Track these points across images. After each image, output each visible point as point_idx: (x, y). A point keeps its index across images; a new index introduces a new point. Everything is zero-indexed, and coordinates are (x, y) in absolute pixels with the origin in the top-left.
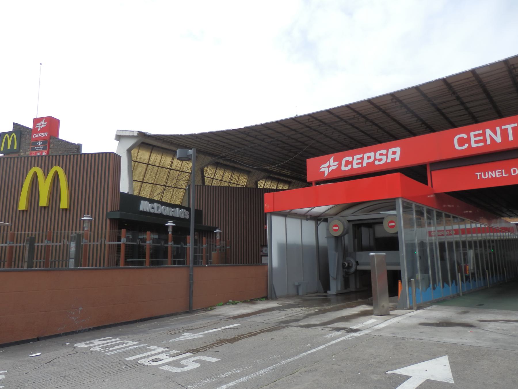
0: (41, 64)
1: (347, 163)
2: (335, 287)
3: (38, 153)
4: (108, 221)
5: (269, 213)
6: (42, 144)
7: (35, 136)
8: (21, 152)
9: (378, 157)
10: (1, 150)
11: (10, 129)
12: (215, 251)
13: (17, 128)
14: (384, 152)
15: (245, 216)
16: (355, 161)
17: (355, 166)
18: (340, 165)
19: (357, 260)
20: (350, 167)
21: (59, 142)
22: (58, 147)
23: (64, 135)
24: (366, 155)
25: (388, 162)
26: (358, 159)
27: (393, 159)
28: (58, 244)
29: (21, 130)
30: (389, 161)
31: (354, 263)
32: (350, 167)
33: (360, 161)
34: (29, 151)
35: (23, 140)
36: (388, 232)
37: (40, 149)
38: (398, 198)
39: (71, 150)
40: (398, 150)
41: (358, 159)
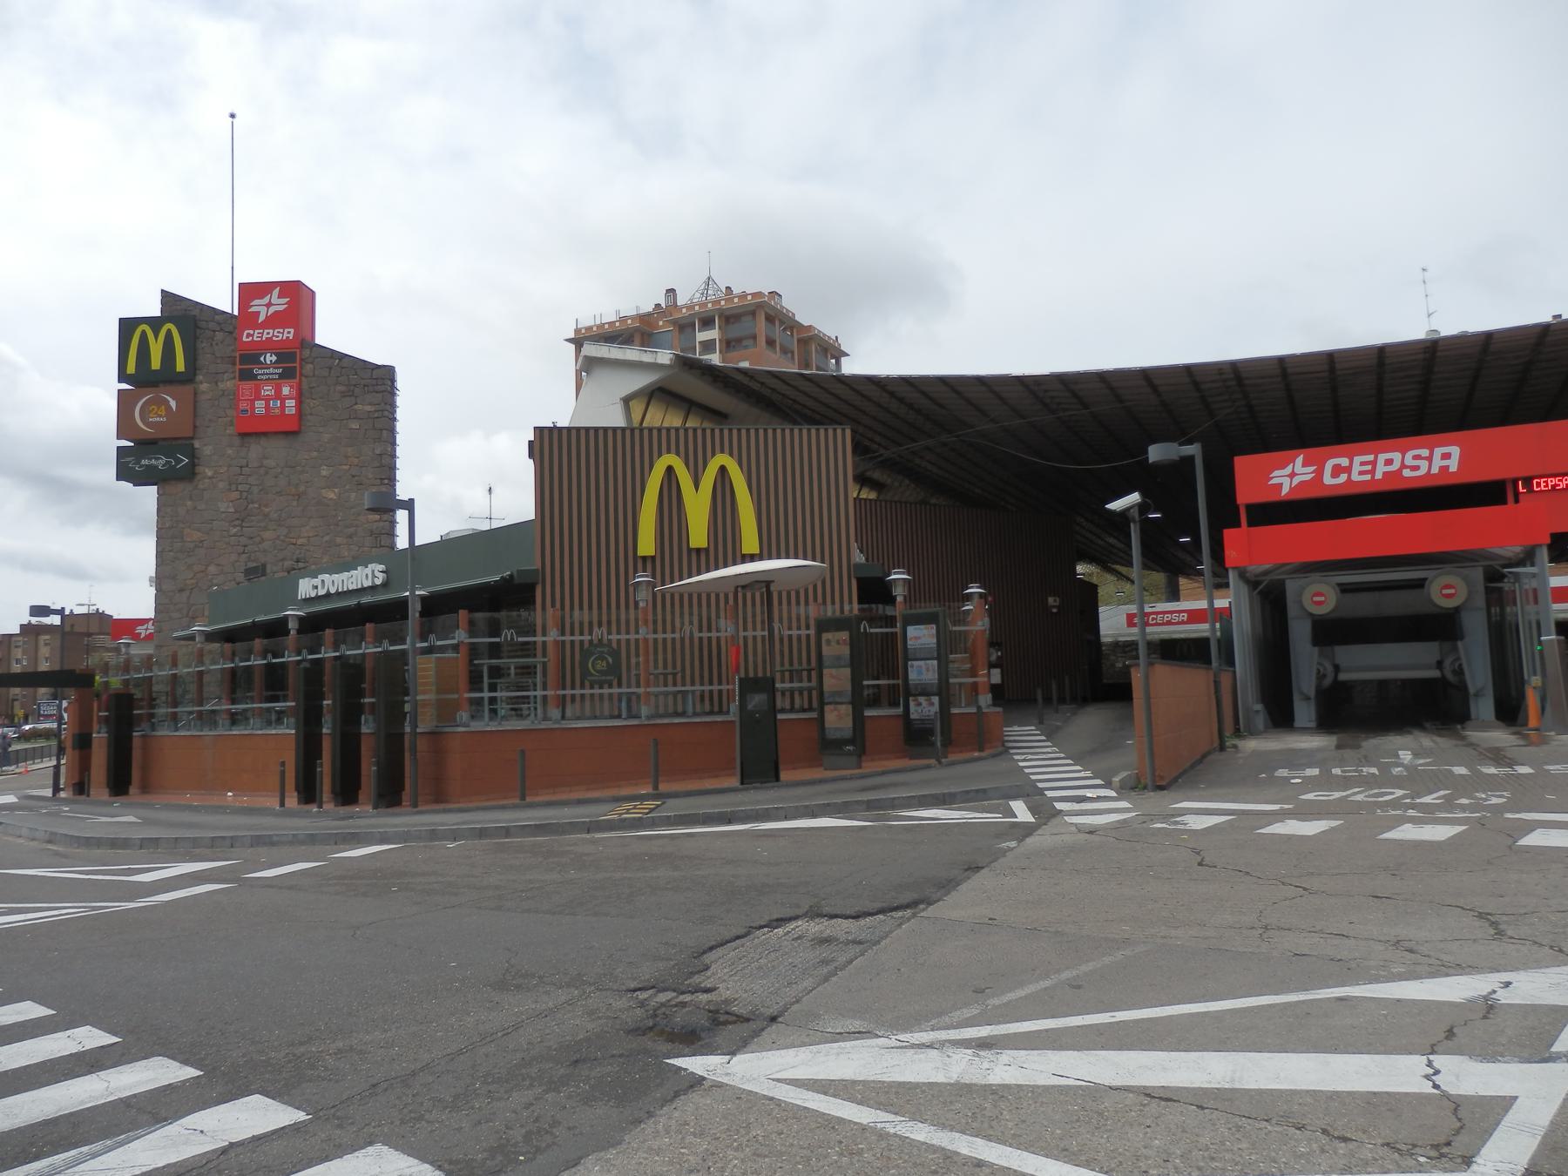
0: (233, 116)
1: (1337, 471)
2: (1304, 712)
4: (854, 583)
5: (1233, 568)
6: (276, 362)
7: (248, 336)
8: (201, 383)
9: (1409, 461)
10: (128, 372)
11: (155, 310)
12: (966, 653)
13: (179, 307)
14: (1425, 452)
15: (921, 577)
16: (1356, 468)
17: (1355, 477)
18: (1319, 473)
19: (1337, 661)
20: (1343, 478)
21: (332, 357)
22: (330, 372)
23: (333, 331)
24: (1382, 457)
25: (1432, 472)
26: (1362, 464)
27: (1444, 469)
28: (669, 636)
29: (195, 316)
30: (1435, 470)
31: (1330, 668)
32: (1343, 478)
33: (1369, 467)
34: (234, 378)
35: (203, 345)
36: (1450, 606)
38: (1540, 546)
39: (377, 385)
40: (1455, 451)
41: (1362, 464)
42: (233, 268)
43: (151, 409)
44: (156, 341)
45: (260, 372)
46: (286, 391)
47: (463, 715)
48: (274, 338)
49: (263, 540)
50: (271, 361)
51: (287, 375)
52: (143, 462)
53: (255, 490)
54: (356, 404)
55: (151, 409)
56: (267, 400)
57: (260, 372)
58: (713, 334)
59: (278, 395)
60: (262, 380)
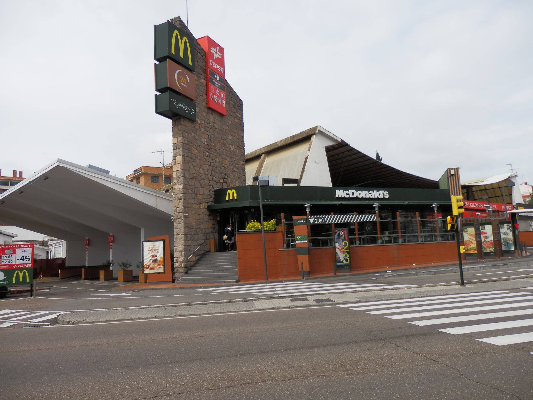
3: (217, 91)
42: (187, 21)
47: (358, 242)
49: (216, 162)
53: (212, 136)
54: (236, 112)
57: (215, 82)
59: (220, 97)
60: (216, 86)
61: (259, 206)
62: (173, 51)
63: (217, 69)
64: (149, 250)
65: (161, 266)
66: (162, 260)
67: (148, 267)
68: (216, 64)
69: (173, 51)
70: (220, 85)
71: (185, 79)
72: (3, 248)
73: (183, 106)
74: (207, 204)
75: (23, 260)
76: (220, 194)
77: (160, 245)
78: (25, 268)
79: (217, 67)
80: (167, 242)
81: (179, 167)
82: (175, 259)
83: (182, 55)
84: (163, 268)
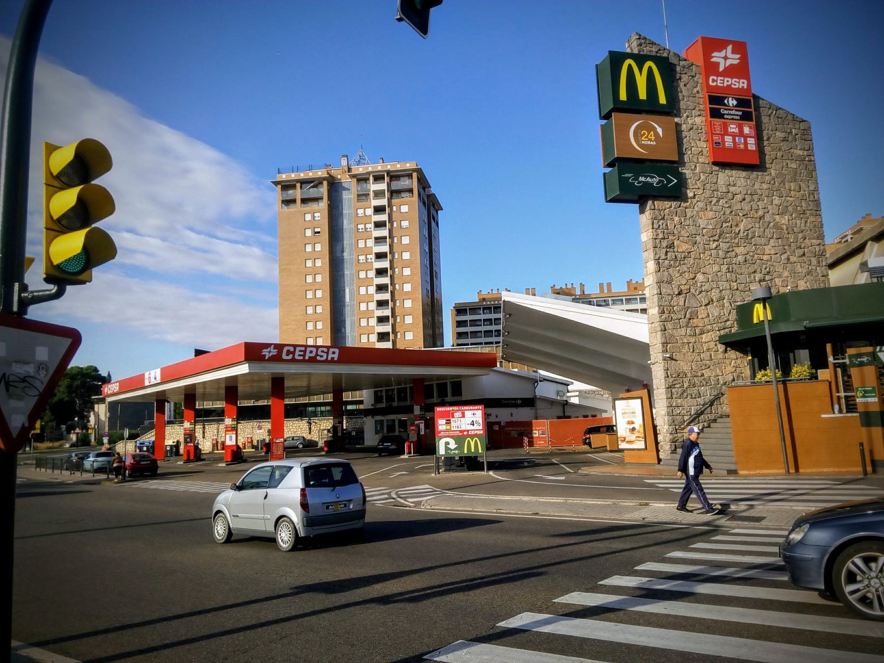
3: (731, 126)
6: (736, 106)
37: (734, 117)
43: (642, 133)
44: (641, 74)
45: (725, 112)
46: (746, 130)
48: (733, 86)
49: (736, 256)
50: (733, 104)
51: (746, 117)
52: (642, 179)
55: (642, 133)
56: (734, 136)
57: (725, 112)
58: (382, 186)
59: (741, 134)
60: (728, 119)
61: (765, 337)
62: (623, 96)
63: (729, 86)
64: (623, 414)
65: (641, 439)
66: (642, 430)
67: (624, 440)
68: (726, 79)
69: (623, 96)
70: (740, 113)
71: (652, 133)
72: (451, 411)
73: (649, 179)
74: (718, 332)
75: (473, 425)
76: (745, 312)
77: (635, 405)
78: (476, 435)
79: (729, 83)
80: (646, 399)
81: (652, 279)
82: (658, 428)
83: (643, 95)
84: (643, 443)
